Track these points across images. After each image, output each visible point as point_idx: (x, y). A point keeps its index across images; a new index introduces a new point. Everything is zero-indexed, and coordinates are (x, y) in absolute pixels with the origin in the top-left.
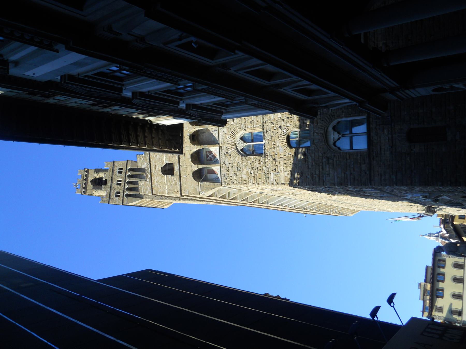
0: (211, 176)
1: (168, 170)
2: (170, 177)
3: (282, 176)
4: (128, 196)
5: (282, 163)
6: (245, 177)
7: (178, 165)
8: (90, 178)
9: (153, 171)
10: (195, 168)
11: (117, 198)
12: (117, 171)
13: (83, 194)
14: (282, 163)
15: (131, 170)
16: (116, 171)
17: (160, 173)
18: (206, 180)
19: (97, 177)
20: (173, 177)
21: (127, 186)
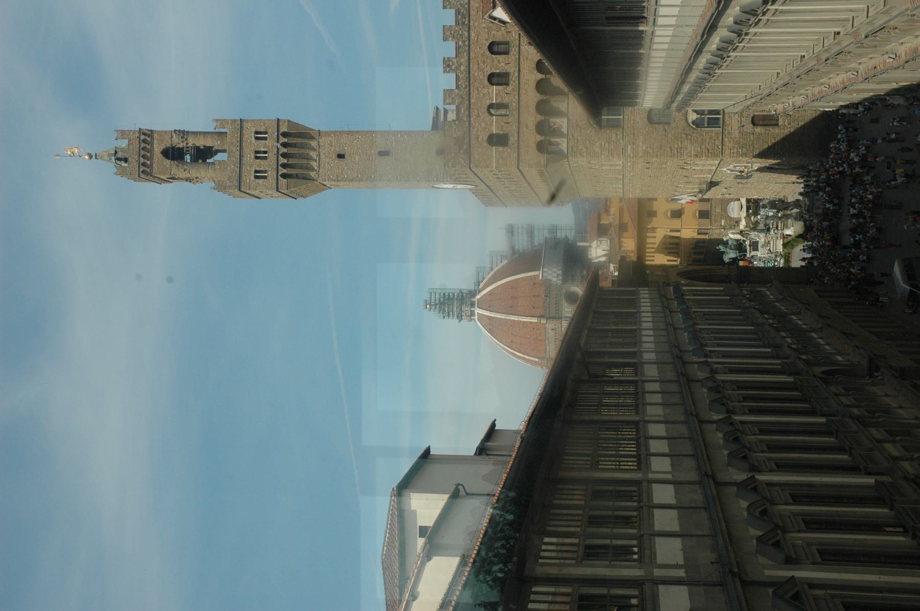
0: (551, 148)
1: (499, 140)
2: (501, 149)
3: (640, 149)
4: (284, 176)
5: (641, 138)
6: (597, 150)
7: (516, 135)
8: (158, 148)
9: (474, 141)
10: (539, 138)
11: (261, 181)
12: (253, 135)
13: (142, 175)
14: (641, 138)
15: (285, 135)
16: (249, 136)
17: (485, 144)
18: (548, 153)
19: (181, 146)
20: (506, 148)
21: (283, 161)
